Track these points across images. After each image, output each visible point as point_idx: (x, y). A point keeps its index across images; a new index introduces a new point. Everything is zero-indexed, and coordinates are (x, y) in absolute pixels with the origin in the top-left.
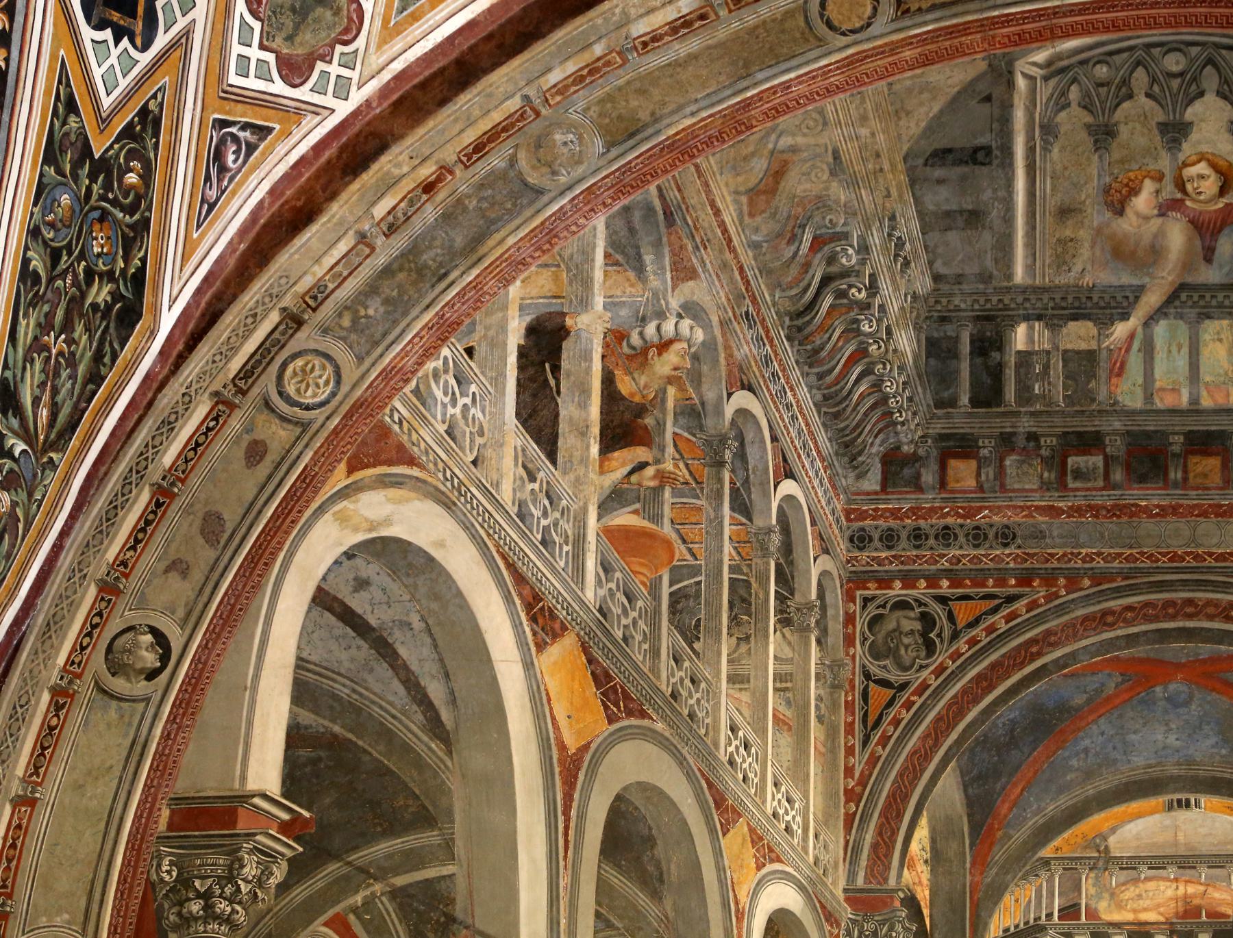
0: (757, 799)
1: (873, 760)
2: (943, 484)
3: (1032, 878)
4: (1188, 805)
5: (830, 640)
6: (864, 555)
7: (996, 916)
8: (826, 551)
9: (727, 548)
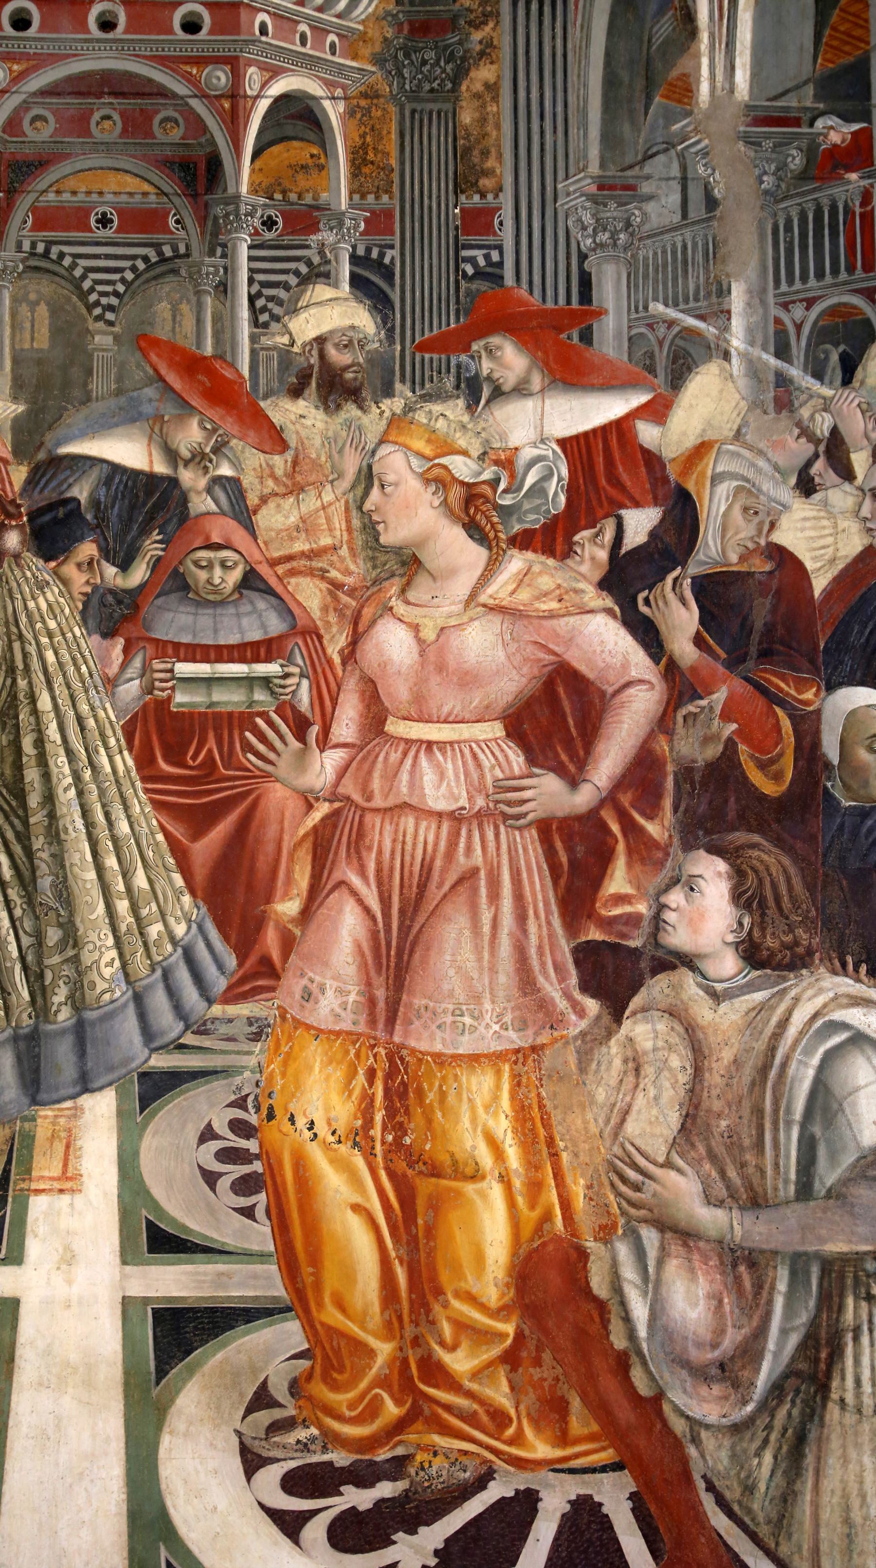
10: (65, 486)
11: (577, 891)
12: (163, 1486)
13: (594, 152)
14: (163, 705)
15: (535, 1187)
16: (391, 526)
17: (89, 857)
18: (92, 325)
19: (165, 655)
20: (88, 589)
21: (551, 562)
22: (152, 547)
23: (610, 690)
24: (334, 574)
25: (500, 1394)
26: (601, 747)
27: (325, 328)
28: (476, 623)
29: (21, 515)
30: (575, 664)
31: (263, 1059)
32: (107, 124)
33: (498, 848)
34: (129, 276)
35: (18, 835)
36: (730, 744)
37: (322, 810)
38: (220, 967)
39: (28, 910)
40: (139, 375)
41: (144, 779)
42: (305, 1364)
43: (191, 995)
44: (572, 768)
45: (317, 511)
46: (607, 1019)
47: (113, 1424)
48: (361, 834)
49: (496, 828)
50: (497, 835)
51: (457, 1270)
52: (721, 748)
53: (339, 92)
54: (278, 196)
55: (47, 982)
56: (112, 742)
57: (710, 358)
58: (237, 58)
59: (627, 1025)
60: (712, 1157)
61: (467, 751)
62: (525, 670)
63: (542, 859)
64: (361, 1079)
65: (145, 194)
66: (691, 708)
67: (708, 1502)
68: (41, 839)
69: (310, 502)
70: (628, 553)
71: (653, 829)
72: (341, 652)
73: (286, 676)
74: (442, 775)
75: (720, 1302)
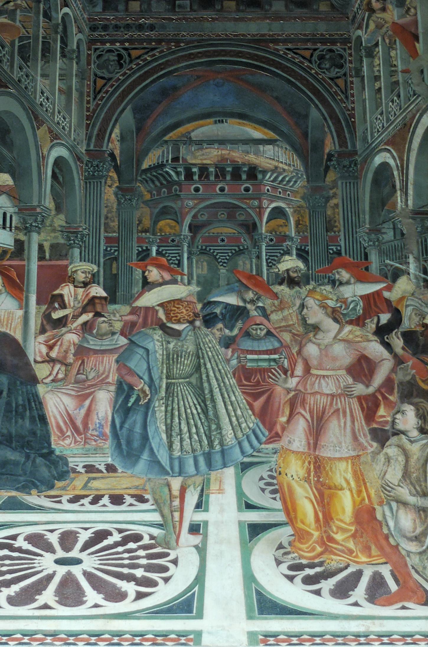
0: (51, 118)
1: (98, 105)
2: (127, 10)
3: (160, 147)
4: (222, 122)
5: (81, 63)
6: (96, 34)
7: (146, 161)
8: (80, 32)
9: (41, 30)
11: (370, 415)
12: (252, 569)
13: (367, 221)
14: (243, 367)
15: (359, 492)
16: (310, 318)
18: (220, 267)
19: (244, 353)
20: (220, 336)
21: (358, 328)
22: (239, 324)
23: (377, 361)
24: (293, 331)
25: (351, 545)
26: (375, 377)
27: (289, 267)
28: (336, 344)
29: (199, 317)
30: (367, 355)
31: (277, 459)
32: (223, 216)
33: (345, 403)
34: (230, 254)
35: (202, 401)
36: (414, 377)
37: (293, 393)
38: (264, 435)
40: (234, 280)
41: (239, 386)
42: (293, 538)
43: (255, 442)
44: (367, 382)
45: (288, 315)
46: (379, 448)
47: (237, 553)
48: (304, 400)
49: (345, 398)
50: (345, 400)
51: (337, 514)
52: (410, 377)
53: (291, 206)
54: (273, 233)
56: (229, 376)
57: (403, 275)
58: (260, 198)
59: (386, 450)
60: (412, 483)
61: (335, 378)
62: (352, 356)
63: (358, 406)
64: (307, 464)
65: (234, 233)
66: (402, 366)
67: (413, 572)
68: (209, 402)
69: (286, 313)
70: (381, 326)
71: (391, 398)
72: (296, 352)
73: (280, 358)
74: (328, 384)
75: (415, 521)
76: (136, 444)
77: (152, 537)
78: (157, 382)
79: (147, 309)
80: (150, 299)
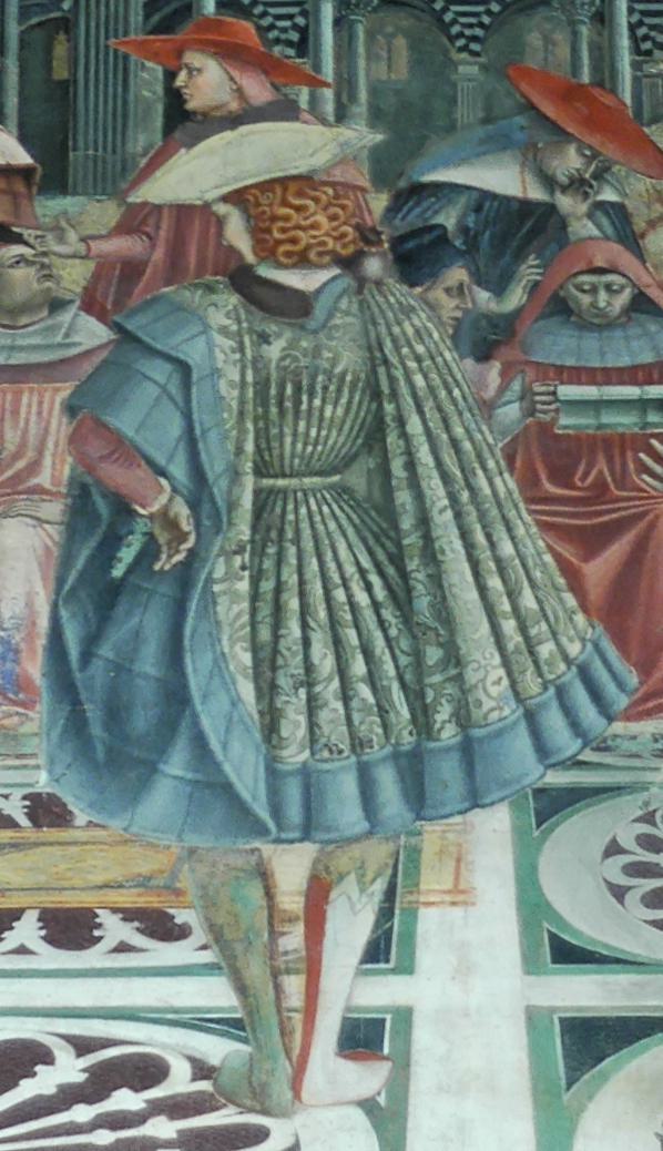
10: (430, 213)
14: (545, 430)
17: (470, 578)
18: (456, 56)
20: (459, 314)
22: (529, 270)
29: (380, 242)
35: (392, 559)
38: (621, 685)
39: (406, 632)
40: (508, 103)
41: (529, 500)
55: (429, 700)
56: (491, 464)
76: (142, 720)
77: (201, 1070)
78: (219, 488)
79: (183, 212)
80: (193, 175)
